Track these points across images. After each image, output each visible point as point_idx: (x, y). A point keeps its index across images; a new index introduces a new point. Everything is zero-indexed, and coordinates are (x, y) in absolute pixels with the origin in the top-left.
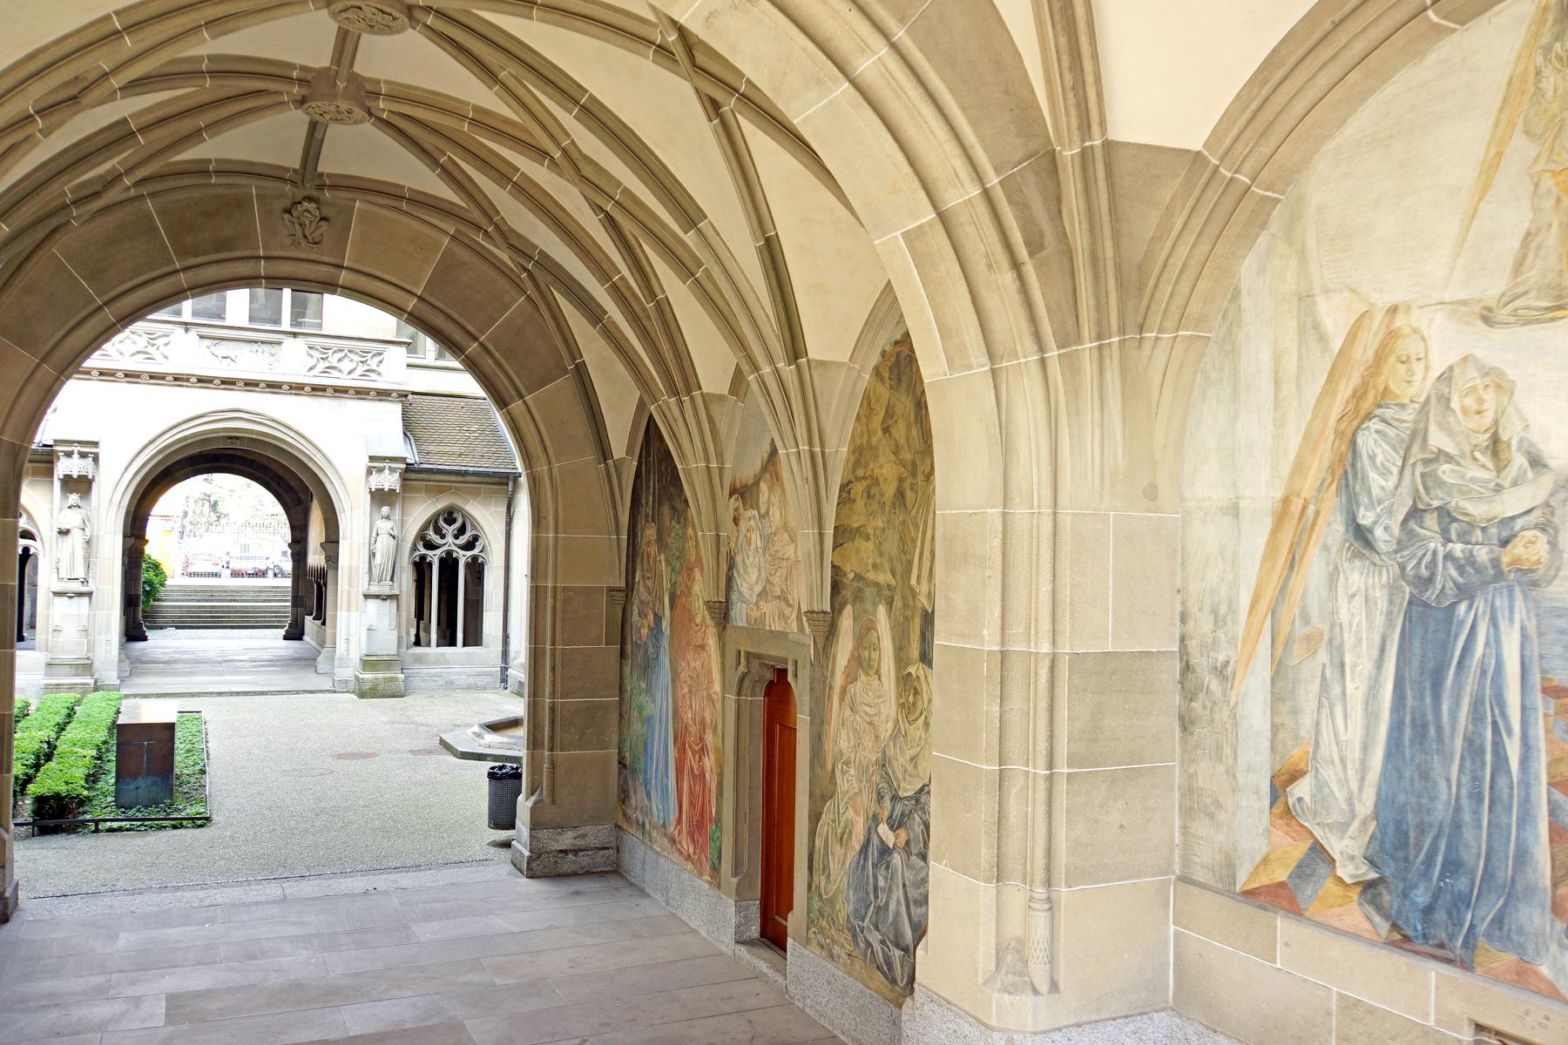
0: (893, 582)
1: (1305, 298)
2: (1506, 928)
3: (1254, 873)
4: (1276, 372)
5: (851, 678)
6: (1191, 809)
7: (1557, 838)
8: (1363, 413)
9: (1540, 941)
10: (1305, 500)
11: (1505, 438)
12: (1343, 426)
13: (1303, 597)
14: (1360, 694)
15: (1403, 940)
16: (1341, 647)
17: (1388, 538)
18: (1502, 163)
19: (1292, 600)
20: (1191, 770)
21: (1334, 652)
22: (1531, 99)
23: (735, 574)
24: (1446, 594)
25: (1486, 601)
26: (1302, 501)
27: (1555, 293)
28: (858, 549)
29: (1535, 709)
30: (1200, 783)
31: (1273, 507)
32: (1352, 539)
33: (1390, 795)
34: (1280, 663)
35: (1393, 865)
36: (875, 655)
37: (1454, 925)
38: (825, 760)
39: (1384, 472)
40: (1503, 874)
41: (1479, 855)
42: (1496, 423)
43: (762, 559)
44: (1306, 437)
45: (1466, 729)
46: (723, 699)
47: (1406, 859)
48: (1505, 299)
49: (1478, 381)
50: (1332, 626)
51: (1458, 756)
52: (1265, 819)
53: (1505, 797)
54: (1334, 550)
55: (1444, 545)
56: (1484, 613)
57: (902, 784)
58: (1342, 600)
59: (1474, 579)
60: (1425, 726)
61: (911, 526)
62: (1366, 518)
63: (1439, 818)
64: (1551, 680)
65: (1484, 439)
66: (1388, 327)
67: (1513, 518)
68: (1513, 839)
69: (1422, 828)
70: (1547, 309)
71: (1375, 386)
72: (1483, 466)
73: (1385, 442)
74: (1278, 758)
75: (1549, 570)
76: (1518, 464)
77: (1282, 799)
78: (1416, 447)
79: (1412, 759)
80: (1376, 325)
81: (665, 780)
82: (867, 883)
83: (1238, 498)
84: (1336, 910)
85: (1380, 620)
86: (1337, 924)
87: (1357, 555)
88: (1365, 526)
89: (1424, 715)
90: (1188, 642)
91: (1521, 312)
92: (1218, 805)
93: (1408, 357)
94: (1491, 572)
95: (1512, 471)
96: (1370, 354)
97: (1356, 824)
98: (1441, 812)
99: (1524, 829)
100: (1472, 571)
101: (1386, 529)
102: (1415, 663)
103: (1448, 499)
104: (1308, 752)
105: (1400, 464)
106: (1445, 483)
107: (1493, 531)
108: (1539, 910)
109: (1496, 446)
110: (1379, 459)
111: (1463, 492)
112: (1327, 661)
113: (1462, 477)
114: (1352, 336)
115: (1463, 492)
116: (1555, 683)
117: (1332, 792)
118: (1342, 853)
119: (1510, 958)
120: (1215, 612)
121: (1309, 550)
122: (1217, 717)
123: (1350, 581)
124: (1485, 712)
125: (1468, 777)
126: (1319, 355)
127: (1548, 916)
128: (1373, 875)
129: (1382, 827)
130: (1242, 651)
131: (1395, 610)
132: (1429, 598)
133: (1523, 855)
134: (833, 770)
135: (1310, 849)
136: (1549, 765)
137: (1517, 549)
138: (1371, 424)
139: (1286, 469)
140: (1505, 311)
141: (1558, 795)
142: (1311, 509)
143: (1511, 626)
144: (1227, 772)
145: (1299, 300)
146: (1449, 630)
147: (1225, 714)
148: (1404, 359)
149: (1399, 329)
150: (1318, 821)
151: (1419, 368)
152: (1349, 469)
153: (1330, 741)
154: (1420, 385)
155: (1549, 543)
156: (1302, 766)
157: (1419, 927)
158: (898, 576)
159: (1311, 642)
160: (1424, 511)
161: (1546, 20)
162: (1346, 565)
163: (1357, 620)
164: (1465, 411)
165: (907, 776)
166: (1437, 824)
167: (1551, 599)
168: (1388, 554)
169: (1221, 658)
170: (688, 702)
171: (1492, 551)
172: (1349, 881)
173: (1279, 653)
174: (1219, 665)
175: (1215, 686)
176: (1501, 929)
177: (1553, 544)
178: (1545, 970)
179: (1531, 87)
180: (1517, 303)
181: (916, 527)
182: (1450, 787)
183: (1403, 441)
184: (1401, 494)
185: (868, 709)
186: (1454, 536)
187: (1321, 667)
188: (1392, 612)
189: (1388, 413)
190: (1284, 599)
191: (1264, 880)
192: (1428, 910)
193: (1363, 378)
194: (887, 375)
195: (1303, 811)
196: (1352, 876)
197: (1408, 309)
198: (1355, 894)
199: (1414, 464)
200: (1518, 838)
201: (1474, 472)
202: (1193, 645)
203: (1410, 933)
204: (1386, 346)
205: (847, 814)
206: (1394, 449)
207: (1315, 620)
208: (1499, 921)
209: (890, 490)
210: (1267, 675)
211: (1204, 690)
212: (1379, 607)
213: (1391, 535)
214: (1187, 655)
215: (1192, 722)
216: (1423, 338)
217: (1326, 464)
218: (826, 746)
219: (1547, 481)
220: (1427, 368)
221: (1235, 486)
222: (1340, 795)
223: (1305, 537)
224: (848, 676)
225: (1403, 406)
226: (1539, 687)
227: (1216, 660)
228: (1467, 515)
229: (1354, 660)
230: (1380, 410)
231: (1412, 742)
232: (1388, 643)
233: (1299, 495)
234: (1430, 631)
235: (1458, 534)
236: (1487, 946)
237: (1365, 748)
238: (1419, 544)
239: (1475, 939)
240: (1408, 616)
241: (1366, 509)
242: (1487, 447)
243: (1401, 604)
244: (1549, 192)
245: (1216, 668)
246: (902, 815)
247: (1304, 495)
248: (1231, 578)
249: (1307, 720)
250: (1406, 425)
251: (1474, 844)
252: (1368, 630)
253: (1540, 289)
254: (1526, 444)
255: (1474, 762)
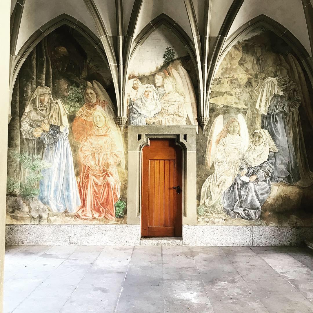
0: (246, 108)
5: (222, 136)
23: (134, 106)
28: (225, 99)
36: (237, 129)
38: (207, 163)
43: (158, 102)
46: (126, 154)
57: (253, 164)
61: (255, 92)
81: (66, 193)
82: (235, 195)
134: (213, 165)
158: (249, 106)
165: (255, 160)
170: (91, 158)
181: (258, 92)
185: (233, 145)
194: (241, 49)
205: (222, 177)
209: (244, 81)
218: (208, 159)
224: (220, 136)
246: (253, 172)
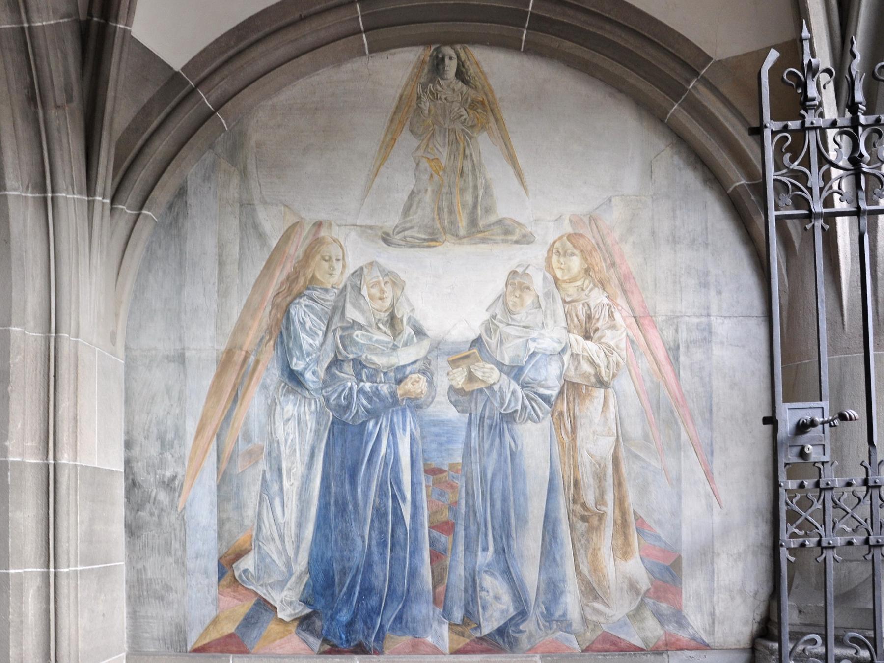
1: (246, 207)
2: (404, 622)
3: (203, 635)
4: (220, 255)
6: (140, 597)
7: (435, 559)
8: (295, 292)
9: (427, 623)
10: (247, 352)
11: (399, 316)
12: (279, 300)
13: (245, 424)
14: (295, 489)
15: (334, 650)
16: (279, 458)
17: (315, 379)
18: (396, 145)
19: (236, 425)
20: (140, 566)
21: (273, 462)
22: (414, 112)
24: (359, 416)
25: (387, 419)
26: (243, 353)
27: (430, 231)
29: (421, 484)
30: (150, 574)
31: (218, 356)
32: (287, 380)
33: (320, 554)
34: (225, 473)
35: (323, 601)
37: (368, 628)
39: (312, 334)
40: (401, 589)
41: (385, 581)
42: (393, 306)
44: (247, 306)
45: (374, 501)
47: (333, 595)
48: (397, 229)
49: (381, 278)
50: (271, 443)
51: (369, 520)
52: (214, 590)
53: (402, 541)
54: (271, 388)
55: (358, 384)
56: (386, 426)
58: (279, 425)
59: (378, 405)
60: (345, 504)
62: (298, 365)
63: (357, 562)
64: (430, 464)
65: (384, 316)
66: (314, 235)
67: (404, 367)
68: (407, 566)
69: (344, 572)
70: (425, 239)
71: (304, 274)
72: (385, 333)
73: (313, 313)
74: (224, 544)
75: (428, 397)
76: (407, 333)
77: (229, 573)
78: (336, 319)
79: (336, 527)
80: (305, 233)
83: (183, 349)
84: (278, 642)
85: (309, 436)
86: (279, 651)
87: (290, 391)
88: (297, 371)
89: (344, 498)
90: (134, 464)
91: (408, 239)
92: (168, 588)
93: (330, 258)
94: (390, 400)
95: (404, 337)
96: (300, 252)
97: (293, 579)
98: (357, 558)
99: (414, 558)
100: (378, 400)
101: (314, 373)
102: (337, 463)
103: (360, 354)
104: (252, 536)
105: (325, 329)
106: (357, 343)
107: (392, 374)
108: (425, 604)
109: (393, 321)
110: (308, 324)
111: (370, 349)
112: (267, 468)
113: (370, 339)
114: (286, 237)
115: (370, 349)
116: (433, 466)
117: (274, 561)
118: (282, 601)
119: (407, 639)
120: (161, 439)
121: (251, 388)
122: (165, 520)
123: (285, 410)
124: (388, 489)
125: (376, 532)
126: (258, 248)
127: (431, 606)
128: (308, 611)
129: (314, 577)
130: (189, 466)
131: (322, 428)
132: (347, 419)
133: (414, 574)
135: (255, 604)
136: (429, 516)
137: (408, 385)
138: (301, 300)
139: (229, 328)
140: (398, 237)
141: (435, 533)
142: (252, 359)
143: (404, 434)
144: (176, 562)
145: (241, 206)
146: (362, 439)
147: (173, 517)
148: (327, 258)
149: (323, 238)
150: (261, 583)
151: (338, 266)
152: (284, 331)
153: (270, 525)
154: (339, 277)
155: (427, 381)
156: (247, 546)
157: (343, 637)
159: (253, 456)
160: (343, 361)
161: (424, 69)
162: (282, 399)
163: (291, 437)
164: (372, 297)
166: (355, 567)
167: (430, 416)
168: (316, 390)
169: (168, 474)
171: (391, 387)
172: (287, 619)
173: (224, 465)
174: (166, 480)
175: (163, 497)
176: (401, 623)
177: (430, 383)
178: (429, 639)
179: (414, 103)
180: (406, 233)
182: (364, 541)
183: (327, 313)
184: (325, 349)
186: (364, 378)
187: (261, 473)
188: (319, 430)
189: (315, 294)
190: (228, 425)
191: (214, 635)
192: (350, 624)
193: (295, 268)
195: (248, 578)
196: (291, 615)
197: (330, 225)
198: (293, 628)
199: (336, 329)
200: (410, 564)
201: (378, 336)
202: (139, 468)
203: (336, 642)
204: (313, 248)
206: (320, 319)
207: (256, 440)
208: (399, 618)
210: (213, 484)
211: (152, 501)
212: (309, 427)
213: (318, 377)
214: (133, 474)
215: (140, 528)
216: (341, 246)
217: (264, 326)
219: (426, 344)
220: (344, 266)
221: (181, 340)
222: (280, 562)
223: (246, 380)
225: (326, 290)
226: (422, 469)
227: (164, 476)
228: (374, 364)
229: (289, 465)
230: (308, 291)
231: (336, 517)
232: (316, 451)
233: (241, 349)
234: (348, 441)
235: (367, 377)
236: (392, 636)
237: (300, 526)
238: (338, 384)
239: (383, 634)
240: (331, 432)
241: (298, 359)
242: (387, 321)
243: (327, 424)
244: (426, 170)
245: (164, 482)
247: (245, 348)
248: (177, 411)
249: (250, 512)
250: (328, 303)
251: (381, 574)
252: (300, 444)
253: (420, 227)
254: (412, 320)
255: (380, 522)
